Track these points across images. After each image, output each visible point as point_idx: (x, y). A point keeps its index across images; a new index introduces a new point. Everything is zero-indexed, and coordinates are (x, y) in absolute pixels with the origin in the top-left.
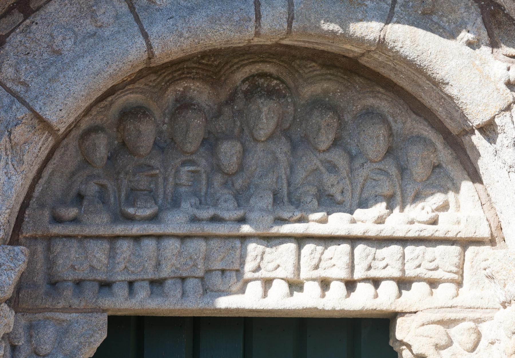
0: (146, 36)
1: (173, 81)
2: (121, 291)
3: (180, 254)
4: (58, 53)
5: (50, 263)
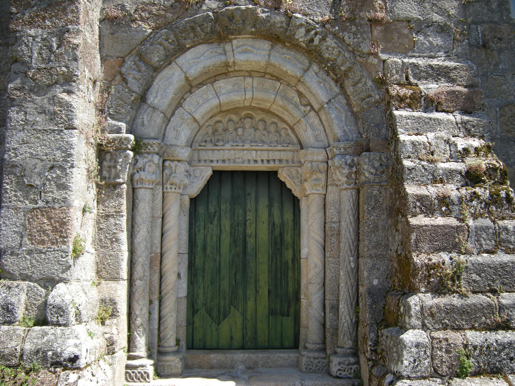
0: (219, 99)
1: (227, 115)
2: (215, 162)
3: (228, 154)
4: (198, 103)
5: (199, 156)
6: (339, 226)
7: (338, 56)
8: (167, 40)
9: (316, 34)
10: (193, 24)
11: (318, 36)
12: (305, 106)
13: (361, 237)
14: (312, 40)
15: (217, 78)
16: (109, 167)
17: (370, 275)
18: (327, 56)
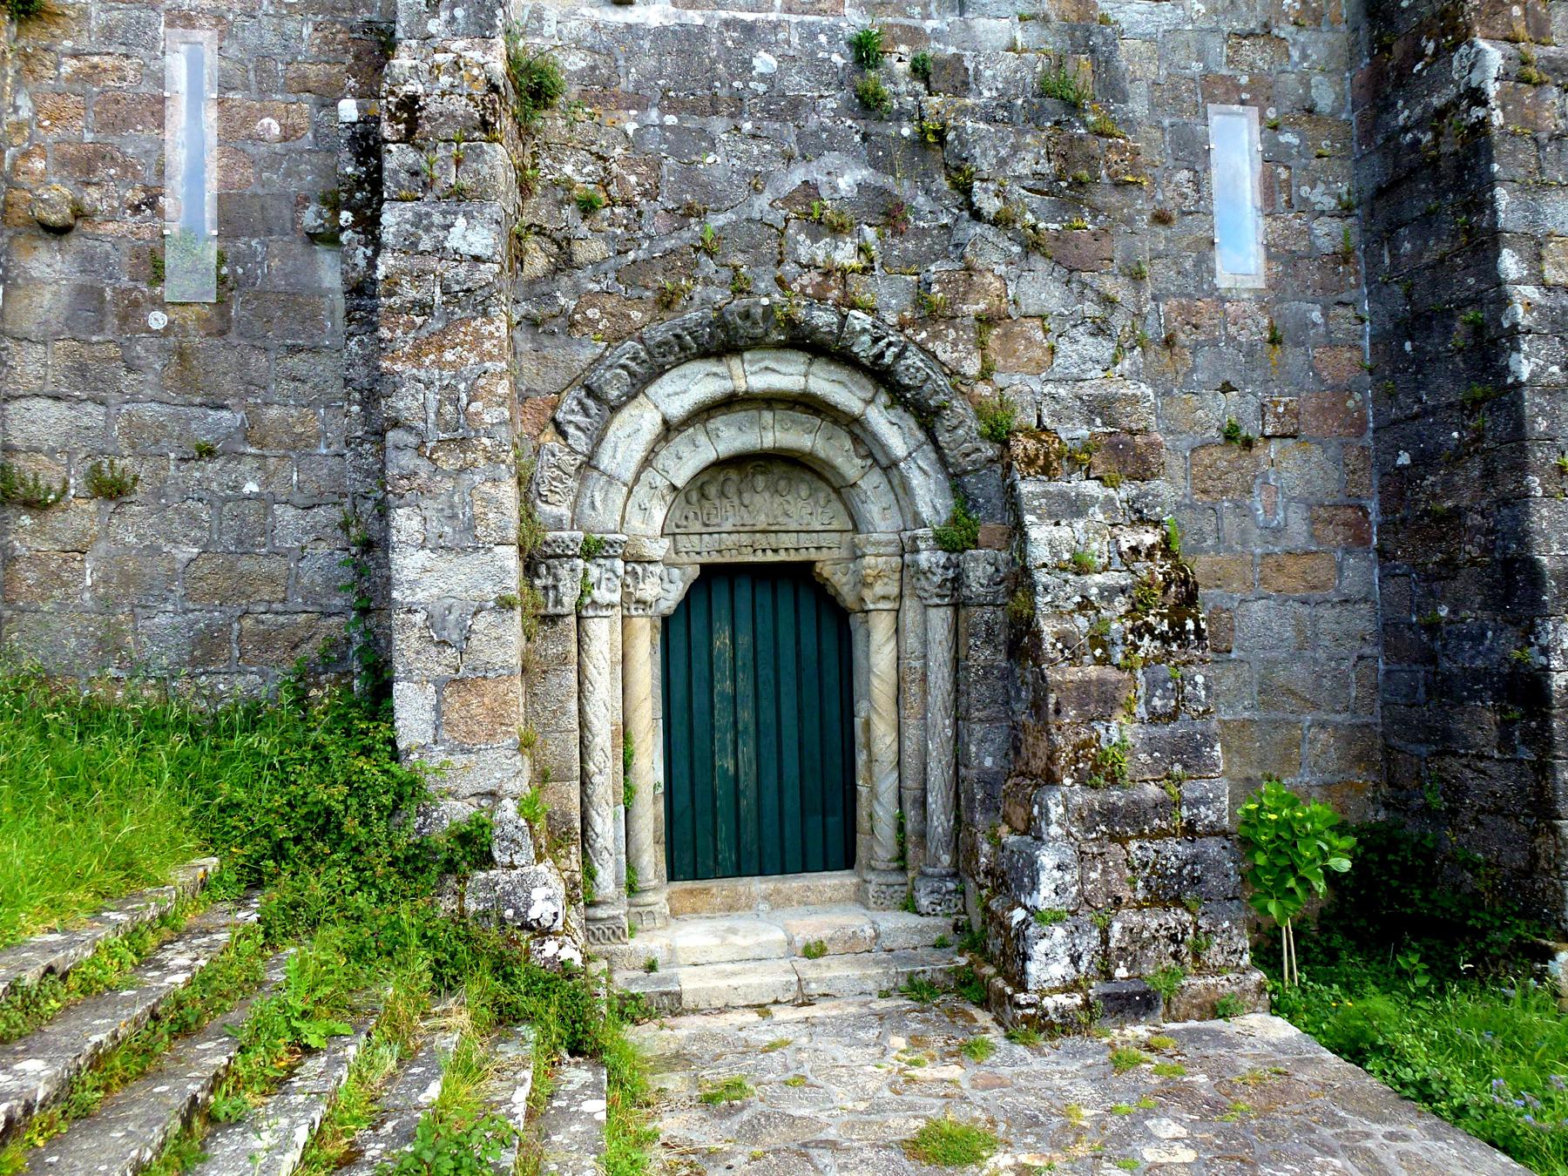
6: (926, 665)
7: (925, 381)
8: (633, 359)
9: (890, 344)
10: (679, 331)
11: (893, 349)
12: (864, 458)
13: (962, 687)
14: (881, 355)
15: (712, 413)
16: (545, 588)
17: (979, 750)
18: (907, 381)
